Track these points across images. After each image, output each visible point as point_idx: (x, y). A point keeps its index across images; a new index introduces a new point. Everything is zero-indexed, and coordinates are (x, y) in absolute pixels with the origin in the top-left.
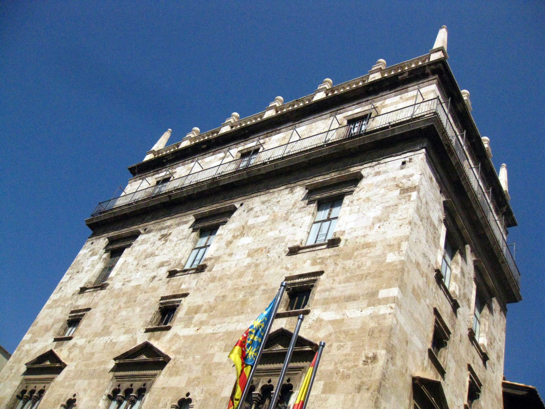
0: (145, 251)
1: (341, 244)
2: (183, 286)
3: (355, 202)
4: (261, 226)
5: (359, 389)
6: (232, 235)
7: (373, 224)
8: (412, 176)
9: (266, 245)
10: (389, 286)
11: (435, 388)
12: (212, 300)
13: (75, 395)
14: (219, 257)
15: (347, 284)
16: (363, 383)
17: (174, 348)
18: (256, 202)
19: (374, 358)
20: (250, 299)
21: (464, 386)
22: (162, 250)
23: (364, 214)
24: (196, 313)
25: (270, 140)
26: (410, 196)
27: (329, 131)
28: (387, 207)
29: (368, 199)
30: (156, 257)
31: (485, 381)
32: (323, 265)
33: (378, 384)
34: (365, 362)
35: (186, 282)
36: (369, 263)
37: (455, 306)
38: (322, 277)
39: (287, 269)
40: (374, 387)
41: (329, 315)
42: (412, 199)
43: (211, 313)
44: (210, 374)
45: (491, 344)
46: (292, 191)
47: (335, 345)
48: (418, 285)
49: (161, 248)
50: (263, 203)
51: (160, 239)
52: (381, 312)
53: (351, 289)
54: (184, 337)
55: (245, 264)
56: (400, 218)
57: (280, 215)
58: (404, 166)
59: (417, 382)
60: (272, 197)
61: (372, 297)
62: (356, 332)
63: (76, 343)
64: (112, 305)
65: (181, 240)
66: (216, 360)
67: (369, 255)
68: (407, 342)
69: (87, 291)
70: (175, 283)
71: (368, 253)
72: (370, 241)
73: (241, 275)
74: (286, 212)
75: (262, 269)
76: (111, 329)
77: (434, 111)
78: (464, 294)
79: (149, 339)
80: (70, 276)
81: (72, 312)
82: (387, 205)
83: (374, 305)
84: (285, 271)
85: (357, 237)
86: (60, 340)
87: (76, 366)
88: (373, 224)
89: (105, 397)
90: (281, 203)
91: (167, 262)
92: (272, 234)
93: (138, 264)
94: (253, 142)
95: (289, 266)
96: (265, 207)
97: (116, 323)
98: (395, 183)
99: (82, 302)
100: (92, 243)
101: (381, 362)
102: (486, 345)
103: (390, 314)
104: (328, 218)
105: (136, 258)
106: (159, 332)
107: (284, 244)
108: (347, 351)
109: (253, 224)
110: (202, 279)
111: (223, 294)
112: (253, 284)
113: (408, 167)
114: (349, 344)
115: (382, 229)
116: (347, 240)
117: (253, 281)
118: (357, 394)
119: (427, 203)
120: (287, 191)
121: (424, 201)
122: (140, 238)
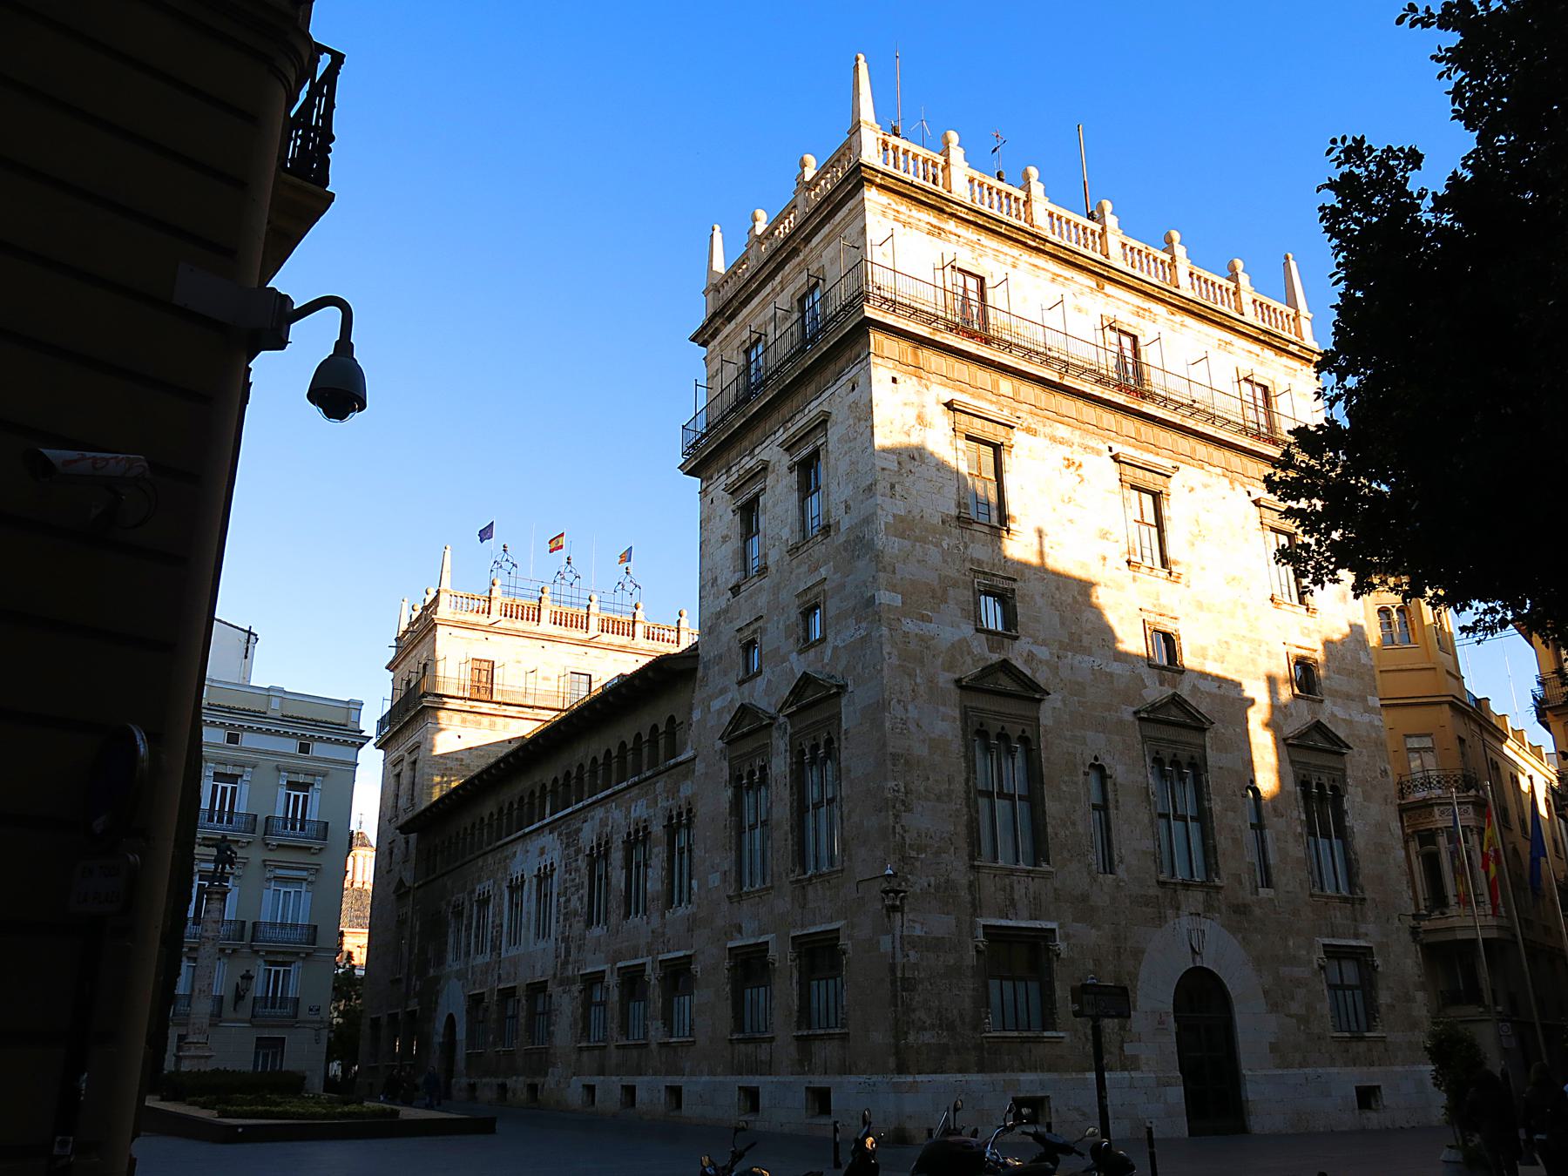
41: (1340, 713)
69: (975, 526)
87: (1063, 701)
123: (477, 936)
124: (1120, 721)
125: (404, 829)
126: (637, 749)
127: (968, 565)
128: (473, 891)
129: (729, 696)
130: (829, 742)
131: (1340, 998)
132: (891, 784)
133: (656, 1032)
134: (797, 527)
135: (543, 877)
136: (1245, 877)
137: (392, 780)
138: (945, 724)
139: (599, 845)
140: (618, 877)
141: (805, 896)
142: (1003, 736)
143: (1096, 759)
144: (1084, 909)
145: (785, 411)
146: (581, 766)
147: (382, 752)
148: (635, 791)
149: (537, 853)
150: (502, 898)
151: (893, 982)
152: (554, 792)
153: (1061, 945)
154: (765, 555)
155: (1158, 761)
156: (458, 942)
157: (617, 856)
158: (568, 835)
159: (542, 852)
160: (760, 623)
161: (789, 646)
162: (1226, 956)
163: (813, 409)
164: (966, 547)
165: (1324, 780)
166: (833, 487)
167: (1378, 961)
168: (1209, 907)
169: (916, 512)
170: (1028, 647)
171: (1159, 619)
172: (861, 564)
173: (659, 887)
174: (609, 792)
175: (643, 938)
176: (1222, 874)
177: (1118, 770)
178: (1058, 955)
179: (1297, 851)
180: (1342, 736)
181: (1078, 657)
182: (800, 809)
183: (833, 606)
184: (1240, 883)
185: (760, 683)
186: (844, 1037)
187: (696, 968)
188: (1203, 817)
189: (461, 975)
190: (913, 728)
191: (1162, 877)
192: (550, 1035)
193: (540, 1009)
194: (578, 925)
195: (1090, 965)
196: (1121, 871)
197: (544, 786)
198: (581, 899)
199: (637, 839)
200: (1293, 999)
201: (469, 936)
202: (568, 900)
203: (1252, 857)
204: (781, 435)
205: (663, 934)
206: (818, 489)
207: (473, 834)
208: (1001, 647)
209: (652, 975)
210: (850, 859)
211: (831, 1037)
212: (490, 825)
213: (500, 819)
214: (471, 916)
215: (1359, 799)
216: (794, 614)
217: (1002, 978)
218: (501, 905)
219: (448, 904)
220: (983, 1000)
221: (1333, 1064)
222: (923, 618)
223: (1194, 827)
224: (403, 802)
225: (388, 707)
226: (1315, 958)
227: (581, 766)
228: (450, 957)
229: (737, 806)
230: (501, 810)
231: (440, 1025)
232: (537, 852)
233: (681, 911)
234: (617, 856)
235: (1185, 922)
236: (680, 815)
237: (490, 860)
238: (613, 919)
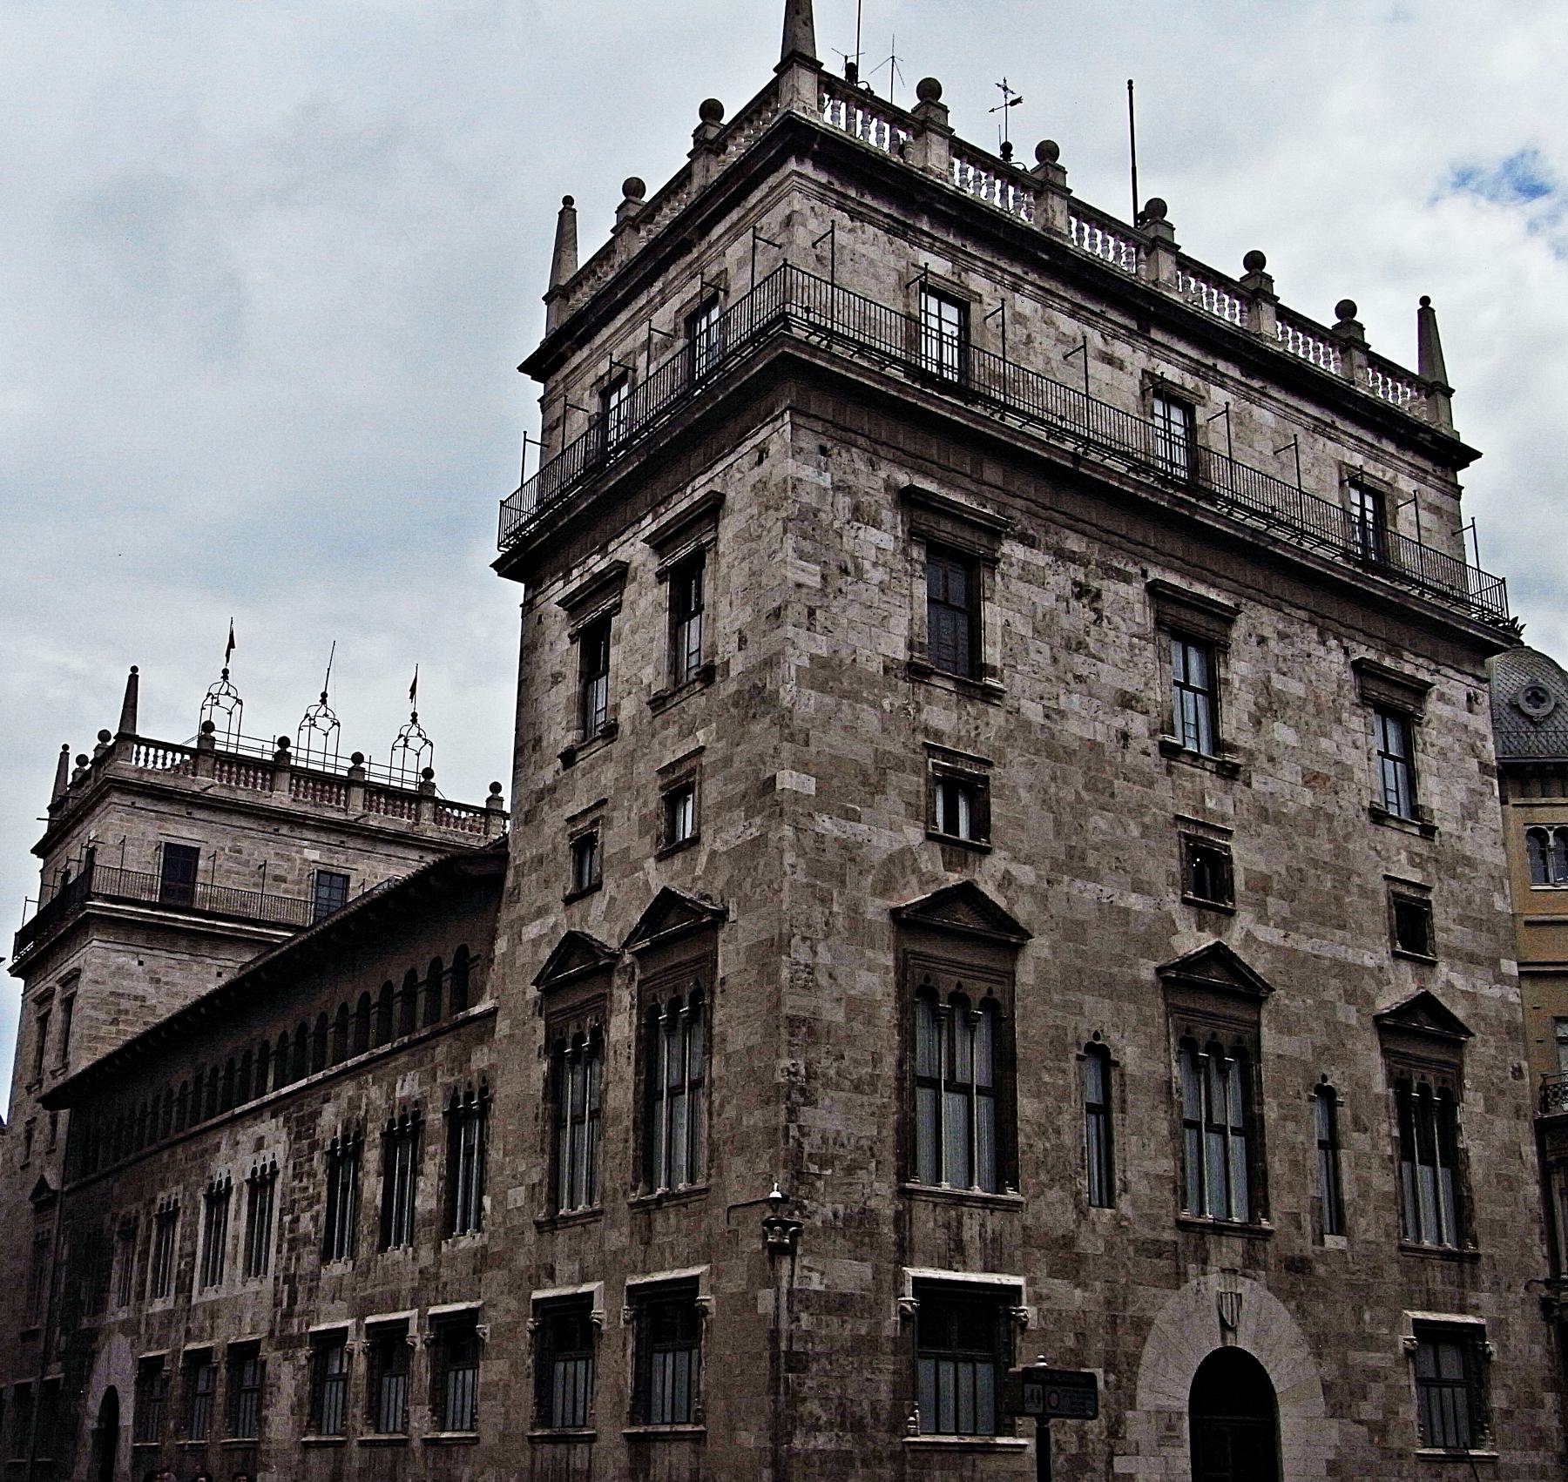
41: (1459, 982)
50: (1282, 636)
69: (936, 681)
87: (1054, 949)
120: (1313, 634)
123: (155, 1270)
124: (1136, 981)
125: (51, 1102)
126: (409, 996)
127: (921, 738)
128: (153, 1201)
129: (551, 920)
130: (697, 995)
131: (1435, 1403)
132: (786, 1062)
133: (421, 1423)
134: (665, 668)
135: (261, 1183)
136: (1307, 1222)
137: (35, 1027)
138: (873, 976)
139: (345, 1138)
140: (372, 1187)
141: (649, 1226)
142: (959, 998)
143: (1097, 1036)
144: (1067, 1259)
145: (659, 489)
146: (323, 1017)
147: (20, 982)
148: (403, 1059)
149: (251, 1148)
150: (196, 1213)
151: (774, 1358)
152: (281, 1053)
153: (1028, 1310)
154: (616, 707)
155: (1188, 1045)
156: (126, 1278)
157: (372, 1157)
158: (300, 1121)
159: (259, 1144)
160: (604, 811)
161: (644, 847)
163: (700, 488)
164: (919, 710)
165: (1431, 1079)
166: (723, 607)
167: (1492, 1346)
168: (1252, 1262)
169: (844, 653)
170: (1003, 865)
171: (1201, 833)
172: (756, 728)
173: (432, 1204)
174: (363, 1057)
175: (407, 1284)
176: (1274, 1214)
177: (1129, 1055)
179: (1383, 1182)
180: (1459, 1012)
181: (1078, 883)
182: (648, 1095)
183: (712, 790)
184: (1299, 1228)
185: (599, 903)
186: (698, 1438)
187: (484, 1328)
188: (1252, 1129)
189: (129, 1328)
190: (823, 980)
191: (1185, 1215)
192: (262, 1422)
193: (248, 1383)
194: (309, 1259)
195: (1070, 1341)
196: (1124, 1204)
197: (266, 1044)
198: (315, 1219)
199: (404, 1134)
200: (1365, 1398)
201: (143, 1271)
202: (296, 1220)
203: (1316, 1188)
204: (649, 526)
205: (437, 1276)
206: (700, 608)
207: (155, 1113)
208: (964, 864)
209: (416, 1337)
210: (720, 1174)
211: (680, 1437)
212: (182, 1101)
213: (197, 1091)
214: (149, 1237)
215: (1480, 1108)
216: (654, 799)
217: (938, 1358)
218: (194, 1224)
219: (113, 1220)
220: (906, 1389)
222: (851, 816)
223: (1236, 1144)
224: (50, 1061)
225: (32, 912)
226: (1401, 1338)
227: (323, 1017)
228: (114, 1299)
229: (554, 1085)
230: (199, 1079)
231: (94, 1405)
232: (250, 1145)
233: (465, 1242)
234: (372, 1157)
235: (1215, 1282)
236: (469, 1096)
237: (180, 1153)
238: (364, 1251)
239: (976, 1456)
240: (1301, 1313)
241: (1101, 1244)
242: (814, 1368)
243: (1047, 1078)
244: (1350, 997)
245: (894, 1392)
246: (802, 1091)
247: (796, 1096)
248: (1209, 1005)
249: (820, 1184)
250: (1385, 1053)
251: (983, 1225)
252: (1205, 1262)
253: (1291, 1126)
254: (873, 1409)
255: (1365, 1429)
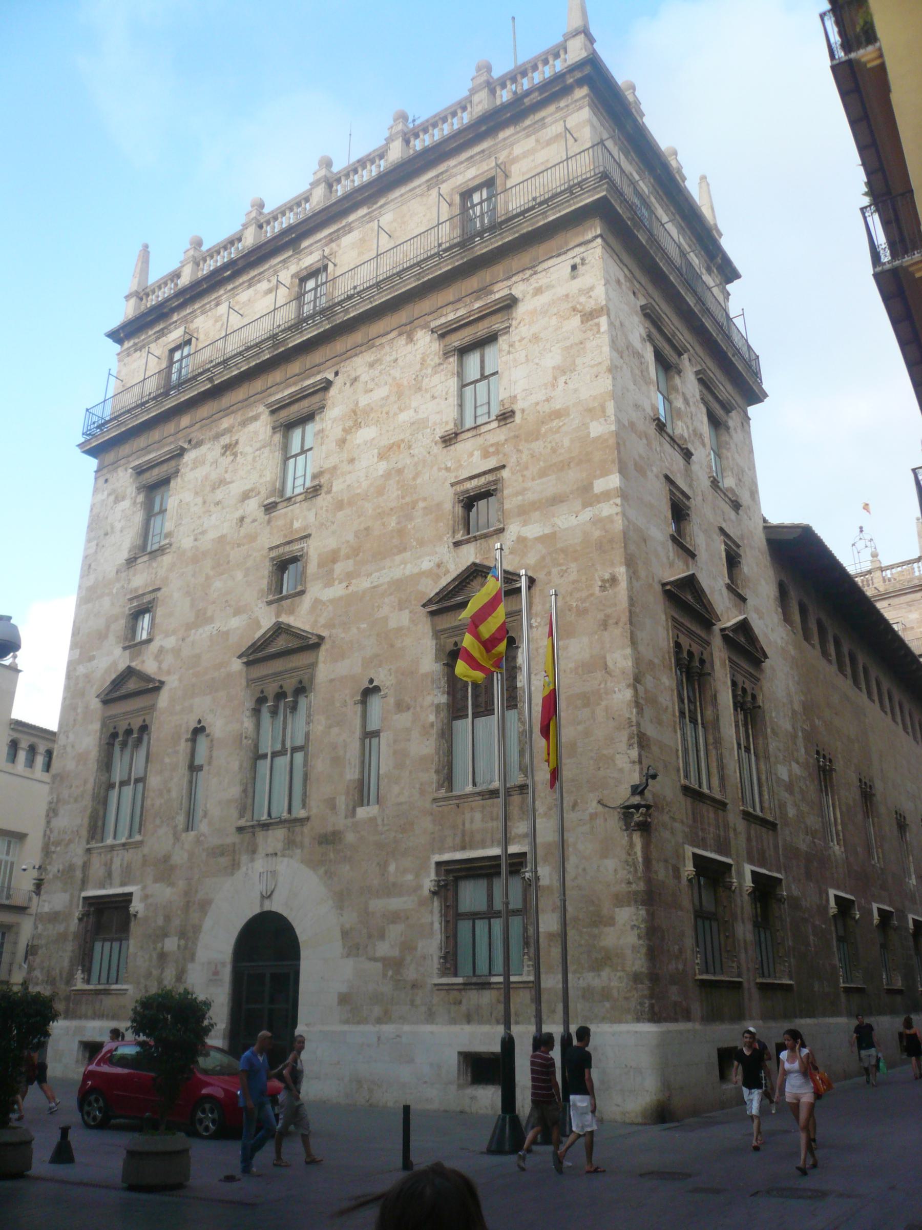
0: (206, 477)
1: (518, 418)
2: (297, 525)
3: (517, 344)
4: (382, 406)
5: (604, 625)
6: (340, 428)
7: (555, 379)
8: (592, 288)
9: (402, 437)
10: (605, 473)
11: (690, 583)
12: (351, 537)
13: (199, 722)
14: (335, 468)
15: (545, 480)
16: (608, 616)
17: (322, 621)
18: (359, 365)
19: (613, 580)
20: (409, 527)
21: (721, 558)
22: (235, 471)
23: (537, 364)
24: (334, 561)
25: (339, 246)
26: (598, 325)
27: (439, 224)
28: (568, 349)
29: (536, 338)
30: (231, 485)
31: (742, 537)
32: (501, 456)
33: (628, 614)
34: (603, 588)
35: (300, 517)
36: (566, 443)
37: (687, 455)
38: (505, 473)
39: (448, 469)
40: (625, 618)
41: (533, 530)
42: (602, 330)
43: (358, 558)
44: (392, 646)
45: (740, 480)
46: (410, 339)
47: (555, 571)
48: (640, 456)
49: (230, 470)
50: (371, 365)
51: (223, 454)
52: (605, 513)
53: (549, 486)
54: (331, 601)
55: (381, 472)
56: (593, 363)
57: (405, 383)
58: (575, 272)
59: (668, 587)
60: (382, 352)
61: (586, 495)
62: (579, 548)
63: (161, 647)
64: (193, 576)
65: (259, 449)
66: (393, 624)
67: (564, 429)
68: (645, 541)
70: (280, 523)
71: (560, 427)
72: (558, 407)
73: (381, 491)
74: (414, 377)
75: (411, 476)
76: (209, 614)
77: (601, 169)
78: (694, 431)
79: (278, 615)
80: (94, 543)
81: (131, 600)
82: (568, 343)
83: (591, 505)
84: (447, 474)
85: (537, 404)
86: (133, 645)
87: (180, 680)
88: (555, 379)
89: (248, 713)
90: (400, 361)
91: (252, 490)
92: (404, 417)
93: (204, 502)
94: (311, 253)
95: (449, 465)
96: (377, 373)
97: (214, 602)
98: (570, 305)
99: (140, 580)
100: (106, 481)
101: (623, 584)
102: (734, 487)
103: (617, 514)
104: (482, 374)
105: (196, 493)
106: (289, 601)
107: (429, 430)
108: (573, 576)
109: (368, 405)
110: (322, 508)
111: (362, 527)
112: (404, 501)
113: (583, 275)
114: (573, 566)
115: (571, 386)
116: (523, 411)
117: (403, 498)
118: (606, 633)
119: (621, 324)
120: (402, 340)
121: (617, 324)
122: (189, 457)
144: (164, 869)
153: (137, 906)
162: (303, 896)
168: (290, 843)
171: (287, 548)
178: (135, 916)
191: (242, 823)
195: (160, 922)
196: (203, 827)
221: (430, 1017)
235: (260, 865)
239: (103, 997)
240: (329, 874)
241: (186, 856)
242: (40, 952)
243: (167, 760)
244: (401, 606)
245: (71, 961)
246: (54, 810)
247: (51, 814)
248: (278, 665)
249: (54, 856)
250: (437, 634)
251: (122, 860)
252: (254, 852)
253: (335, 730)
254: (61, 974)
255: (379, 965)
